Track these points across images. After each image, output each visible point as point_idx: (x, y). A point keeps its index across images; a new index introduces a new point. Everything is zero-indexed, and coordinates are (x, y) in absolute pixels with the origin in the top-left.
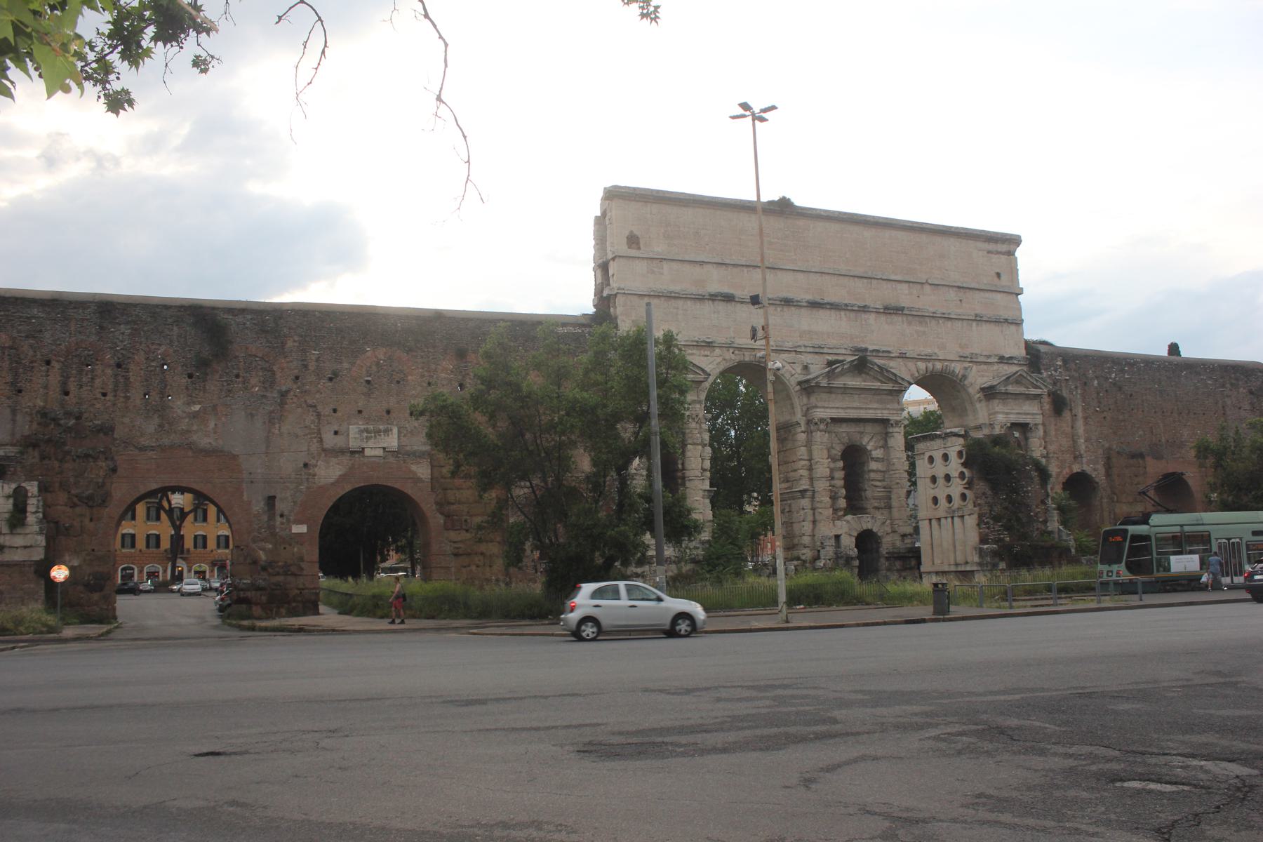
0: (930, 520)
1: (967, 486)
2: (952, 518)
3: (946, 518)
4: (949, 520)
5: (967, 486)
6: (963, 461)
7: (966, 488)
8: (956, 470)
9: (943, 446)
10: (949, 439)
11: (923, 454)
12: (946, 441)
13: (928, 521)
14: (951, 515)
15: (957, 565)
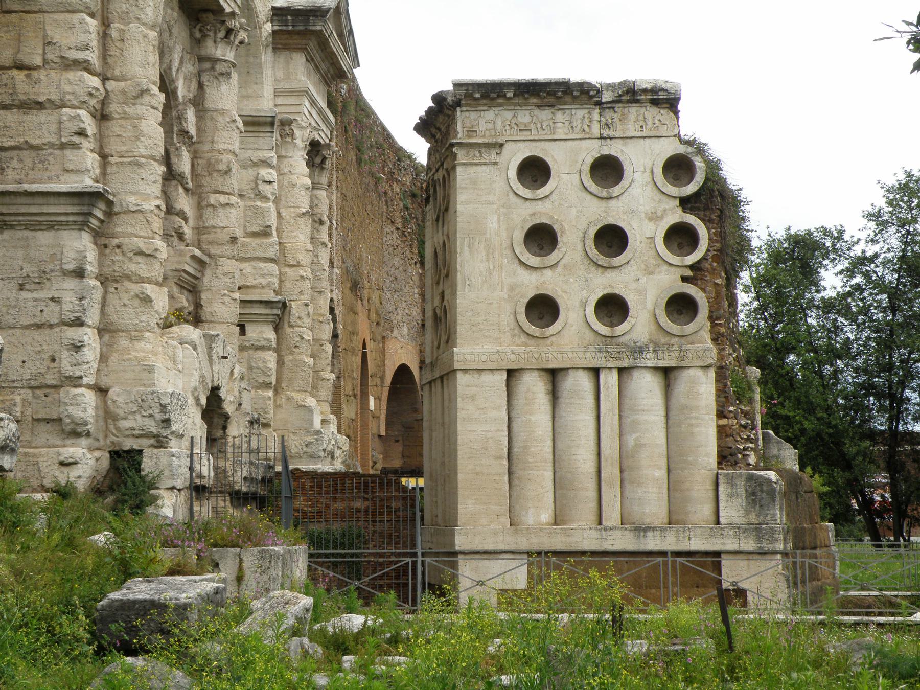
1: (689, 273)
3: (596, 372)
5: (689, 273)
6: (691, 189)
7: (684, 279)
8: (654, 217)
10: (633, 111)
11: (501, 145)
12: (609, 114)
13: (504, 376)
14: (625, 364)
15: (641, 529)
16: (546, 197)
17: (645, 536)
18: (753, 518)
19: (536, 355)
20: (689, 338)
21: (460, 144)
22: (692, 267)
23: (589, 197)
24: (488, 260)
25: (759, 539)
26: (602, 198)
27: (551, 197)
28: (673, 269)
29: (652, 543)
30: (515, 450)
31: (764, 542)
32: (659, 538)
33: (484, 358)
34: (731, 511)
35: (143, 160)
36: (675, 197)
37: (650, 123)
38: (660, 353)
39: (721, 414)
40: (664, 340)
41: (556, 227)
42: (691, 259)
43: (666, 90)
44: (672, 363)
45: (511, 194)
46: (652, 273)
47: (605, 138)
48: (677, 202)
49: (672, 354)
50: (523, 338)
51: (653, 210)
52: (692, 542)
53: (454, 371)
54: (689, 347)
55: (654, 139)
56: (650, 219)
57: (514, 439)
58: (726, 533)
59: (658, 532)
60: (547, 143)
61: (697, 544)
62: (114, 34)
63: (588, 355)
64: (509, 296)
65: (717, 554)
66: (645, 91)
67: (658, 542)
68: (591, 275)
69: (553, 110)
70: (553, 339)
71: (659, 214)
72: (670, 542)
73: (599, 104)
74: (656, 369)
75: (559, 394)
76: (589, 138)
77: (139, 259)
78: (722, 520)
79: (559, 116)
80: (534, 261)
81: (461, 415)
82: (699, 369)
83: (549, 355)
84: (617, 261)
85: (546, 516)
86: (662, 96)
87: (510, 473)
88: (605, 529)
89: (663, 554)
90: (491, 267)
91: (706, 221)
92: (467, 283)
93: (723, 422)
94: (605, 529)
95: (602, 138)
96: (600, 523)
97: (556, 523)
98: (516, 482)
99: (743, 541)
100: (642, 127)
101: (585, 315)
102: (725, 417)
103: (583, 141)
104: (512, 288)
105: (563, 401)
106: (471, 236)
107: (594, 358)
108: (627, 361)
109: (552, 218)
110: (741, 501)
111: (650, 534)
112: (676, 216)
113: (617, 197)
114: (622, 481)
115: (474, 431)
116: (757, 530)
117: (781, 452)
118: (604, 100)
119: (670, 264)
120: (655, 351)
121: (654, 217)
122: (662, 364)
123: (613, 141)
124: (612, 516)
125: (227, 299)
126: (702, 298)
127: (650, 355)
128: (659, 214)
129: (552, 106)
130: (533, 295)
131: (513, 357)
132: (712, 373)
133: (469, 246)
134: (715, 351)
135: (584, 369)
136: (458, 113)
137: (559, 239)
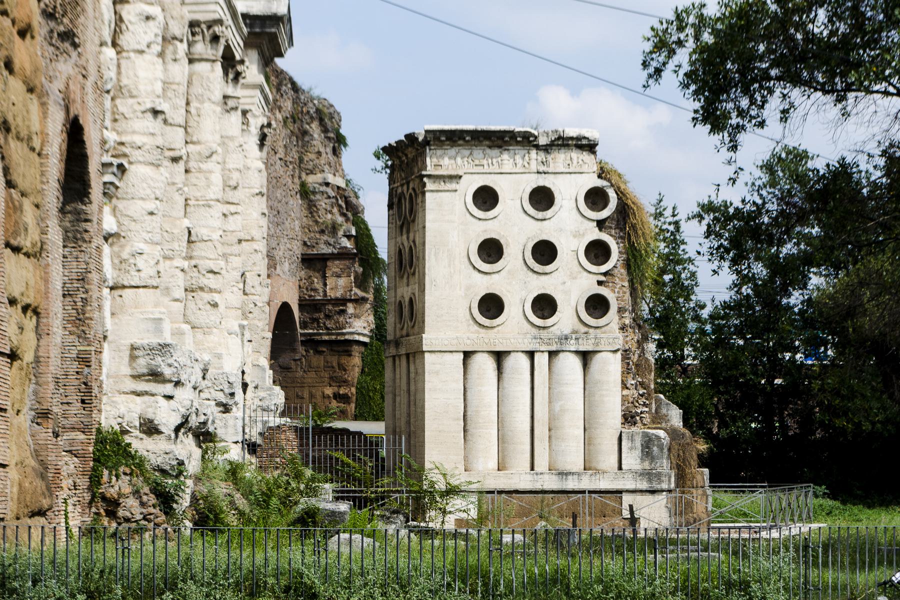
0: (467, 355)
1: (602, 278)
2: (552, 354)
3: (531, 354)
4: (542, 360)
5: (602, 278)
7: (600, 283)
8: (577, 235)
9: (534, 167)
11: (460, 177)
13: (461, 356)
15: (563, 474)
16: (495, 217)
17: (566, 479)
18: (647, 465)
19: (486, 341)
20: (603, 329)
21: (429, 176)
22: (605, 274)
23: (528, 218)
24: (449, 266)
25: (650, 481)
26: (538, 220)
27: (498, 217)
28: (591, 276)
29: (571, 484)
30: (469, 413)
31: (654, 483)
32: (577, 480)
33: (446, 342)
34: (632, 460)
35: (212, 203)
36: (594, 220)
37: (575, 162)
38: (580, 340)
39: (624, 386)
40: (584, 329)
41: (502, 241)
42: (604, 268)
43: (588, 138)
44: (590, 348)
45: (468, 215)
46: (575, 278)
47: (541, 173)
48: (595, 224)
49: (589, 341)
50: (476, 327)
51: (577, 230)
52: (601, 483)
53: (423, 352)
54: (602, 336)
55: (577, 175)
56: (575, 236)
57: (469, 405)
58: (626, 476)
59: (576, 477)
60: (496, 175)
61: (604, 484)
62: (193, 110)
63: (526, 341)
64: (466, 295)
65: (620, 492)
66: (572, 138)
67: (576, 484)
68: (529, 279)
69: (500, 150)
70: (500, 328)
71: (581, 232)
72: (586, 483)
73: (537, 147)
74: (577, 352)
75: (504, 370)
76: (529, 173)
77: (210, 275)
78: (624, 467)
79: (505, 156)
80: (485, 267)
81: (427, 386)
82: (609, 353)
83: (497, 341)
84: (548, 268)
85: (493, 464)
86: (584, 142)
87: (465, 431)
88: (537, 474)
89: (583, 492)
90: (452, 271)
91: (619, 238)
92: (434, 283)
93: (626, 392)
94: (537, 474)
95: (538, 173)
96: (532, 469)
97: (499, 470)
98: (469, 437)
99: (639, 482)
100: (569, 165)
101: (524, 310)
102: (627, 388)
103: (524, 175)
104: (468, 288)
105: (506, 375)
106: (437, 247)
107: (530, 343)
108: (555, 345)
109: (499, 234)
110: (638, 452)
111: (570, 477)
112: (595, 234)
113: (550, 219)
114: (550, 437)
115: (438, 399)
116: (648, 475)
117: (669, 412)
118: (540, 144)
119: (590, 272)
120: (577, 339)
121: (577, 235)
122: (582, 348)
123: (547, 175)
124: (542, 464)
125: (235, 289)
126: (612, 298)
127: (573, 342)
128: (581, 232)
129: (500, 147)
130: (484, 294)
131: (468, 342)
132: (619, 355)
133: (435, 255)
134: (621, 338)
135: (523, 352)
136: (428, 150)
137: (504, 251)
